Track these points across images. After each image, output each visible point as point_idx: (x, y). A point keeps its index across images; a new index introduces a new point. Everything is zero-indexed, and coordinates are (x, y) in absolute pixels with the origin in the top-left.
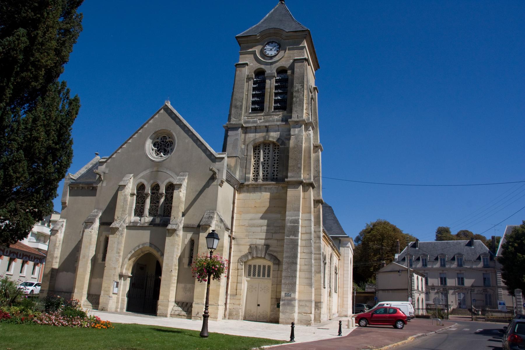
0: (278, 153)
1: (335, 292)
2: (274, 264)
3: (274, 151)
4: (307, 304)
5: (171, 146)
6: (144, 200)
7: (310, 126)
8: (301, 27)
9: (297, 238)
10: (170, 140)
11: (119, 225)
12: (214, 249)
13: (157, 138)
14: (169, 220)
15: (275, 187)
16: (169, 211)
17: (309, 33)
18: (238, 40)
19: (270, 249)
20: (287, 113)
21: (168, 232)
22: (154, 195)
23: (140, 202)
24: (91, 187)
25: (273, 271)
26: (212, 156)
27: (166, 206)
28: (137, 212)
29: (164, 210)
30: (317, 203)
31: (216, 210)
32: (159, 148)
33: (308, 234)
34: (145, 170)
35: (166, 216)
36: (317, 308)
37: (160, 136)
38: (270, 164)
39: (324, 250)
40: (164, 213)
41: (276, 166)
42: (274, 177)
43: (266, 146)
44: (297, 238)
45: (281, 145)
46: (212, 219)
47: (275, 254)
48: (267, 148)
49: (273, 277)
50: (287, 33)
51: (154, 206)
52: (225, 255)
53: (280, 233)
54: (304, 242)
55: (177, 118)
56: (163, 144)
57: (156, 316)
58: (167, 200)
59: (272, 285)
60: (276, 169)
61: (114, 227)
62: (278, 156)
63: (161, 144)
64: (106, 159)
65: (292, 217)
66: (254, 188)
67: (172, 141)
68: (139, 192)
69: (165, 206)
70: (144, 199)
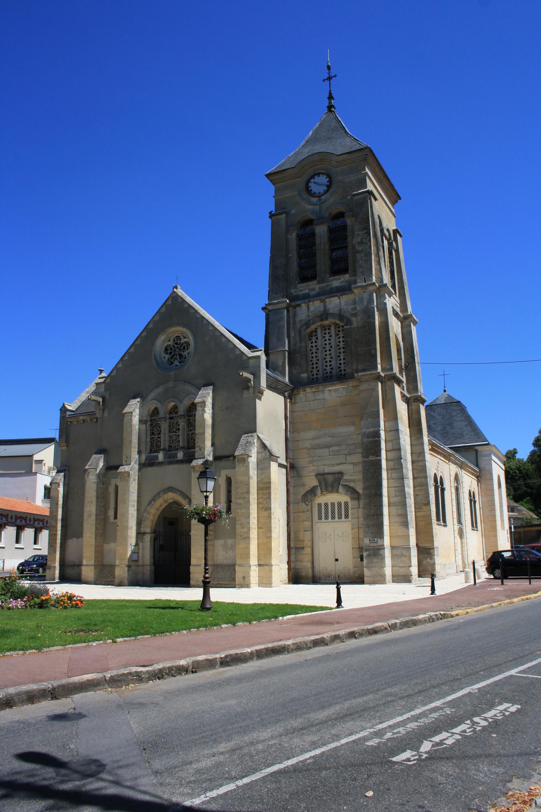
0: (343, 337)
1: (473, 530)
2: (352, 499)
3: (338, 335)
4: (405, 552)
5: (188, 348)
7: (385, 292)
8: (358, 145)
9: (378, 458)
10: (185, 340)
11: (130, 468)
12: (209, 492)
13: (168, 339)
14: (194, 452)
15: (343, 388)
17: (371, 151)
18: (270, 179)
19: (345, 477)
20: (350, 276)
21: (194, 470)
22: (172, 421)
24: (94, 418)
25: (352, 509)
26: (244, 355)
27: (190, 434)
28: (153, 446)
29: (188, 440)
30: (414, 402)
31: (256, 432)
32: (173, 353)
33: (396, 451)
34: (157, 387)
35: (192, 449)
36: (429, 557)
37: (172, 336)
38: (333, 355)
39: (437, 470)
40: (189, 443)
41: (342, 357)
42: (341, 373)
43: (325, 330)
44: (378, 458)
45: (346, 324)
46: (251, 445)
47: (352, 485)
48: (327, 331)
49: (352, 518)
50: (337, 158)
51: (174, 436)
52: (275, 494)
53: (356, 453)
54: (391, 463)
55: (191, 308)
56: (177, 347)
57: (189, 587)
58: (191, 425)
59: (352, 530)
60: (342, 362)
61: (123, 471)
62: (343, 341)
63: (174, 347)
64: (104, 379)
65: (369, 428)
66: (314, 392)
67: (188, 342)
68: (153, 418)
69: (188, 435)
70: (160, 428)
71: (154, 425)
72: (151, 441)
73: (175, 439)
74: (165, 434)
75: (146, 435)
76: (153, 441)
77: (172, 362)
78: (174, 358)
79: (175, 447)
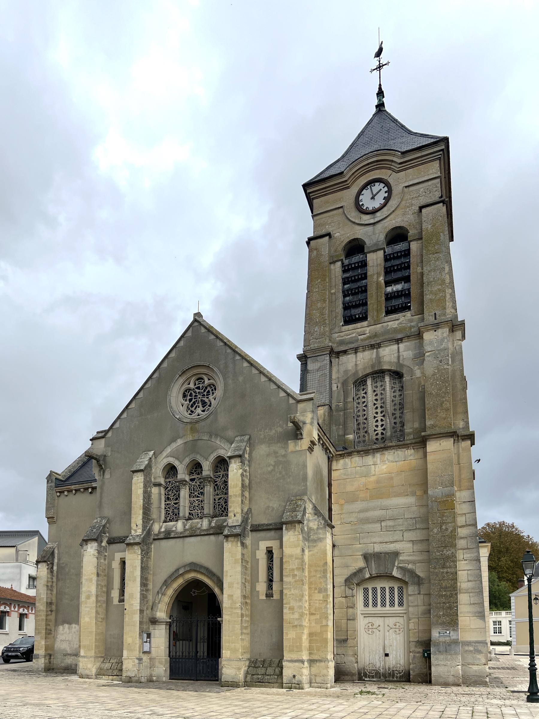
6: (177, 493)
16: (222, 507)
22: (193, 484)
23: (172, 498)
27: (217, 499)
28: (169, 514)
29: (214, 507)
32: (193, 400)
51: (197, 502)
58: (218, 488)
70: (177, 491)
72: (165, 508)
73: (197, 505)
74: (185, 498)
75: (160, 499)
76: (169, 508)
77: (192, 412)
78: (195, 406)
79: (198, 515)
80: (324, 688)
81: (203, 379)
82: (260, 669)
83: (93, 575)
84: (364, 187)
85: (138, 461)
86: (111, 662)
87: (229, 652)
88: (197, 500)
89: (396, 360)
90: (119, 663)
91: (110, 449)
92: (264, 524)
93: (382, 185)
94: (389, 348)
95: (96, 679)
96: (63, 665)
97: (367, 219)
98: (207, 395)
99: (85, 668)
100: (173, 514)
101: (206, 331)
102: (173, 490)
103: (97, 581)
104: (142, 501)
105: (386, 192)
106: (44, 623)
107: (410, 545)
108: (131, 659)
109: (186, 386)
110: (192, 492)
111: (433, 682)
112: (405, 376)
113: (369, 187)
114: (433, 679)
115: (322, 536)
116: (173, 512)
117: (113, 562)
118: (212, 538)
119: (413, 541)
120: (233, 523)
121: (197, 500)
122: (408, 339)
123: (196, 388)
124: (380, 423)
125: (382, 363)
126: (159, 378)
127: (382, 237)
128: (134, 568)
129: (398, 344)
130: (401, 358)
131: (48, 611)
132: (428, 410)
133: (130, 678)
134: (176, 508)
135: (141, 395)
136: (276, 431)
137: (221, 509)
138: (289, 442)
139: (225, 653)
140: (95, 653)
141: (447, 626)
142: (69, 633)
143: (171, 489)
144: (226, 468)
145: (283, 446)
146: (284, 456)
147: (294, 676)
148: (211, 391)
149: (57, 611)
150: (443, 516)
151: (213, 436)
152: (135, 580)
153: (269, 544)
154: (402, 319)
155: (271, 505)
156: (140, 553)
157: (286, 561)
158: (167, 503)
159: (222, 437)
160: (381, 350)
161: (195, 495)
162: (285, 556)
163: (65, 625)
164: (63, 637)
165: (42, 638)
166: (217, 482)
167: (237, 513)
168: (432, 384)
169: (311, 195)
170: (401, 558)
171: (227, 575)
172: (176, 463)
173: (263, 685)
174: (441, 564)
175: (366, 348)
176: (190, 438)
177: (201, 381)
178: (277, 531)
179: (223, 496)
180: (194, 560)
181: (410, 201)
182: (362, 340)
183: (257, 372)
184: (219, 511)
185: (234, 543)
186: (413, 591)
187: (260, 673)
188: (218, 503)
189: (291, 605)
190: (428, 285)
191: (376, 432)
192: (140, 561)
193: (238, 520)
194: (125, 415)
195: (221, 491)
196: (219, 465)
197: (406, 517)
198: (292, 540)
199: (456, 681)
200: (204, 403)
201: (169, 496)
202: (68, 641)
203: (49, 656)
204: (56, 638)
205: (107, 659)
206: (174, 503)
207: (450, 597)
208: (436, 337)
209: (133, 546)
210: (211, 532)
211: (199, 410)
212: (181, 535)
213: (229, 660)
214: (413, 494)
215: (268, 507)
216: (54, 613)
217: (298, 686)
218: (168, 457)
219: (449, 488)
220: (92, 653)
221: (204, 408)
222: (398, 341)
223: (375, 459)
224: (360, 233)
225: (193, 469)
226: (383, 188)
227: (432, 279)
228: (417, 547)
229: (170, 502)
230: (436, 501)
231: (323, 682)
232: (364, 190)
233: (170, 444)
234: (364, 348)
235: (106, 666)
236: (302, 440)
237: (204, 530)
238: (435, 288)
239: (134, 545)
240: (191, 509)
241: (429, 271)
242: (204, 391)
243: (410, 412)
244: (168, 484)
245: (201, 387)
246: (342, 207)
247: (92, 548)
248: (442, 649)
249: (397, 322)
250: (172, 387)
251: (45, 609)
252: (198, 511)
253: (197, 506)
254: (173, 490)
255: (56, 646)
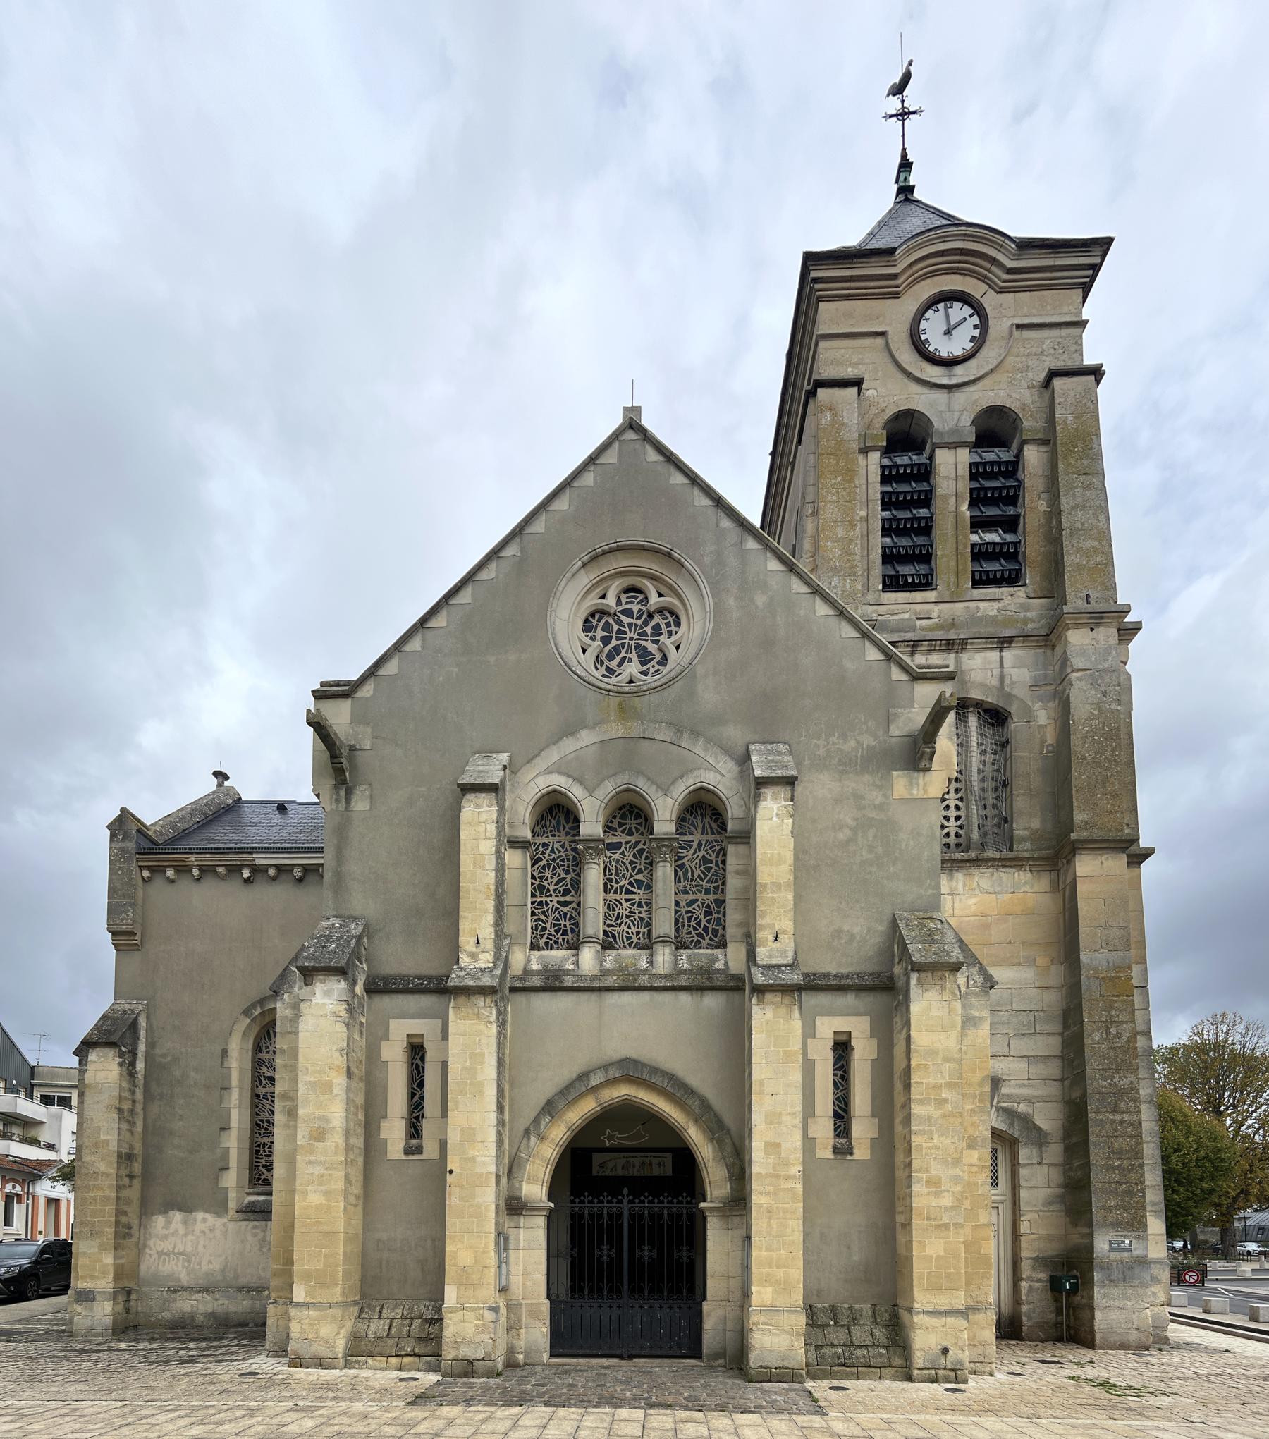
6: (569, 877)
23: (552, 888)
27: (683, 904)
29: (677, 922)
32: (614, 643)
40: (677, 930)
51: (625, 905)
71: (544, 862)
72: (533, 914)
73: (627, 913)
76: (543, 913)
80: (983, 1373)
81: (640, 592)
82: (831, 1330)
83: (333, 1074)
84: (932, 303)
85: (467, 768)
86: (384, 1315)
87: (770, 1289)
88: (627, 901)
89: (995, 682)
90: (412, 1320)
91: (369, 730)
92: (829, 974)
93: (967, 311)
94: (983, 654)
95: (345, 1367)
96: (167, 1315)
97: (934, 373)
98: (653, 635)
99: (310, 1336)
100: (557, 932)
101: (662, 459)
102: (554, 868)
103: (348, 1090)
104: (493, 874)
105: (975, 327)
106: (110, 1208)
107: (1023, 1065)
108: (473, 1310)
109: (592, 602)
110: (613, 877)
111: (1097, 1342)
112: (1015, 720)
113: (941, 306)
114: (1098, 1336)
115: (976, 1014)
116: (555, 925)
117: (383, 1043)
118: (685, 998)
119: (1028, 1057)
120: (770, 956)
121: (627, 901)
122: (1023, 642)
123: (622, 612)
124: (952, 813)
125: (969, 685)
126: (521, 563)
127: (967, 420)
128: (477, 1059)
129: (1001, 651)
130: (1007, 681)
131: (121, 1177)
132: (1077, 791)
133: (470, 1362)
134: (565, 915)
135: (465, 596)
136: (858, 742)
137: (695, 929)
138: (895, 773)
139: (759, 1293)
140: (343, 1293)
141: (1125, 1229)
142: (186, 1235)
143: (549, 865)
144: (707, 825)
145: (878, 782)
146: (880, 808)
147: (945, 1351)
148: (663, 626)
149: (147, 1177)
150: (1111, 1008)
151: (686, 735)
152: (478, 1093)
153: (842, 1023)
154: (1008, 600)
155: (846, 928)
156: (493, 1018)
157: (918, 1066)
158: (539, 899)
159: (709, 740)
160: (964, 656)
161: (622, 887)
162: (917, 1051)
163: (171, 1213)
164: (166, 1246)
165: (103, 1248)
166: (682, 858)
167: (785, 932)
168: (1085, 738)
169: (817, 286)
170: (1004, 1090)
171: (761, 1092)
172: (576, 793)
173: (852, 1374)
174: (1109, 1103)
175: (935, 645)
176: (616, 730)
177: (636, 598)
178: (863, 994)
179: (700, 896)
180: (634, 1055)
181: (1024, 359)
182: (922, 629)
183: (804, 589)
184: (690, 933)
185: (783, 1010)
186: (1029, 1158)
187: (836, 1342)
188: (687, 912)
189: (933, 1173)
190: (1071, 534)
191: (946, 830)
192: (494, 1041)
193: (785, 951)
194: (415, 645)
195: (693, 883)
196: (688, 816)
197: (1015, 1007)
198: (934, 1012)
199: (1144, 1339)
200: (645, 656)
201: (545, 883)
202: (182, 1254)
203: (126, 1292)
204: (145, 1246)
205: (372, 1308)
206: (558, 902)
207: (1130, 1171)
208: (1093, 643)
209: (474, 999)
210: (683, 983)
211: (633, 668)
212: (596, 984)
213: (772, 1310)
214: (1031, 962)
215: (839, 932)
216: (137, 1183)
217: (953, 1374)
218: (550, 773)
219: (1121, 954)
220: (336, 1294)
221: (645, 668)
222: (1003, 642)
223: (954, 883)
224: (922, 401)
225: (615, 817)
226: (971, 316)
227: (1079, 525)
228: (1039, 1070)
229: (548, 899)
230: (1098, 978)
231: (981, 1359)
232: (930, 311)
233: (557, 742)
234: (931, 645)
235: (373, 1328)
236: (928, 774)
237: (661, 977)
238: (1087, 545)
239: (474, 994)
240: (608, 922)
241: (1073, 508)
242: (646, 623)
243: (1024, 795)
244: (541, 849)
245: (635, 612)
246: (883, 334)
247: (327, 993)
248: (1116, 1275)
249: (996, 605)
250: (560, 588)
251: (113, 1171)
252: (629, 927)
253: (628, 917)
254: (554, 868)
255: (143, 1268)
